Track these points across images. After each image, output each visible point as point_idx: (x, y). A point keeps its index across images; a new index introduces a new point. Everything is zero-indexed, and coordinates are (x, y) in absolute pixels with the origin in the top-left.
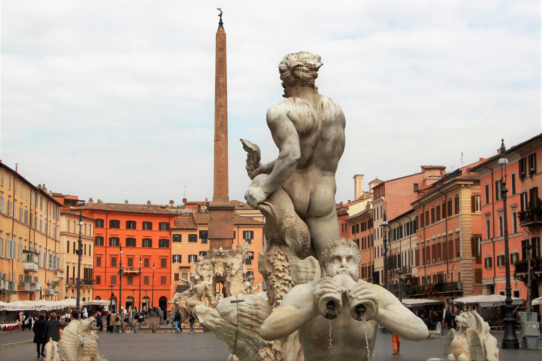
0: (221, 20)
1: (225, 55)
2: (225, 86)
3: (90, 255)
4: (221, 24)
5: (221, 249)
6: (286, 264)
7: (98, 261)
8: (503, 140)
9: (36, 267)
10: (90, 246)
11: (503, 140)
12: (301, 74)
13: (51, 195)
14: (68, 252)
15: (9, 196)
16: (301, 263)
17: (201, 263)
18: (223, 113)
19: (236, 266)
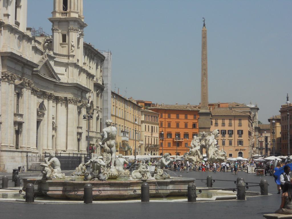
0: (204, 23)
1: (206, 40)
2: (206, 55)
3: (157, 132)
4: (204, 25)
5: (204, 132)
6: (105, 155)
7: (161, 135)
8: (288, 94)
9: (127, 139)
10: (157, 127)
11: (288, 94)
12: (108, 124)
13: (135, 103)
14: (146, 130)
15: (114, 106)
16: (108, 154)
17: (195, 139)
18: (205, 68)
19: (211, 141)
